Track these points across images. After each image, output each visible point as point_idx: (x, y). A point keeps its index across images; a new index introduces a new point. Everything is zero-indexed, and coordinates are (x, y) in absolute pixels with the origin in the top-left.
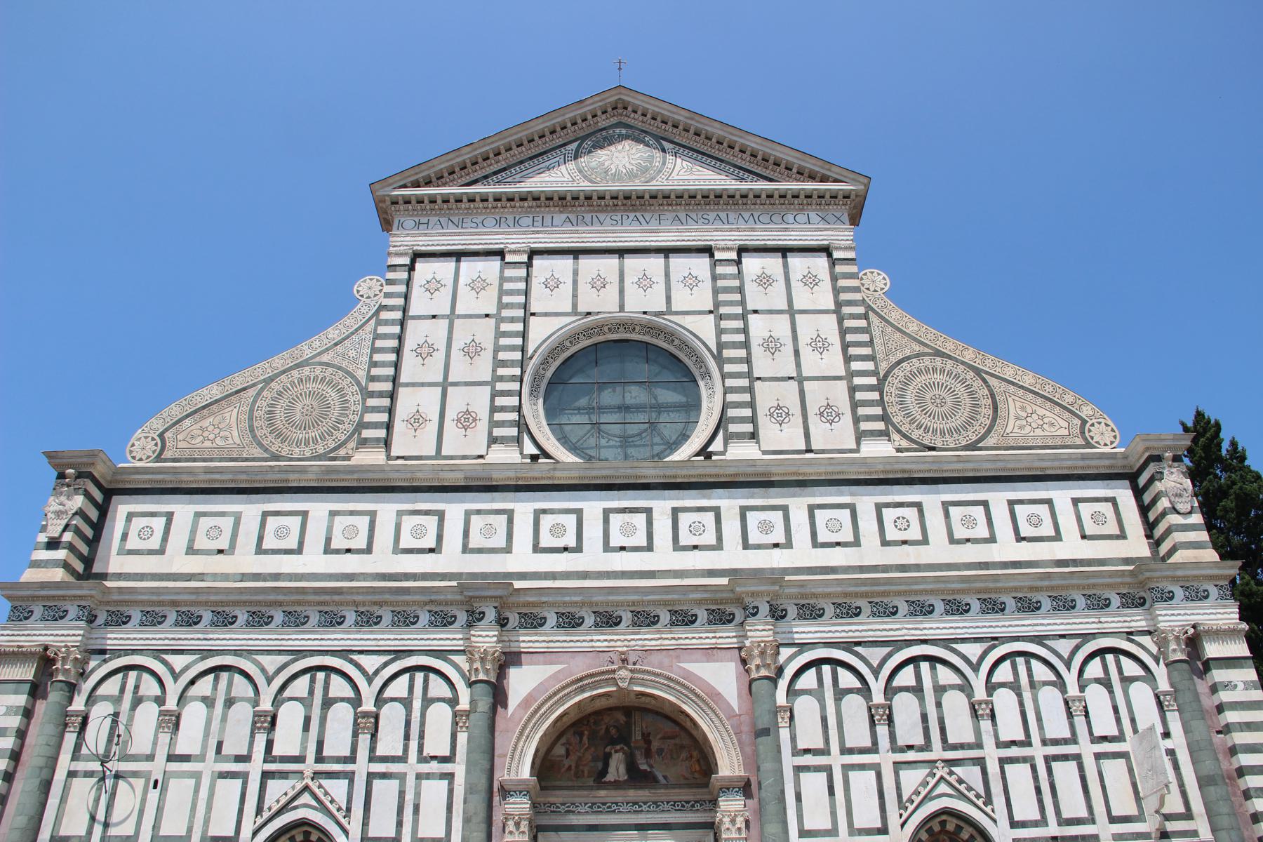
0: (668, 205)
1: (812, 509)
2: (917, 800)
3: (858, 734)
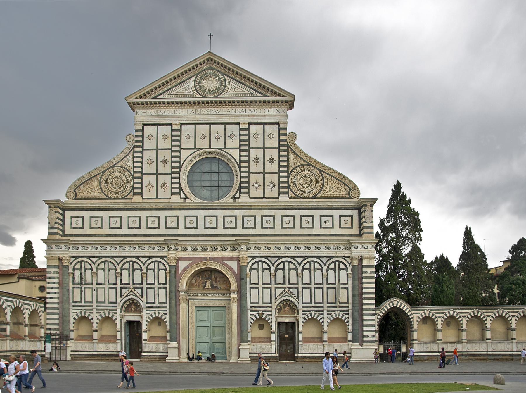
0: (226, 105)
1: (262, 216)
2: (280, 297)
3: (267, 280)
